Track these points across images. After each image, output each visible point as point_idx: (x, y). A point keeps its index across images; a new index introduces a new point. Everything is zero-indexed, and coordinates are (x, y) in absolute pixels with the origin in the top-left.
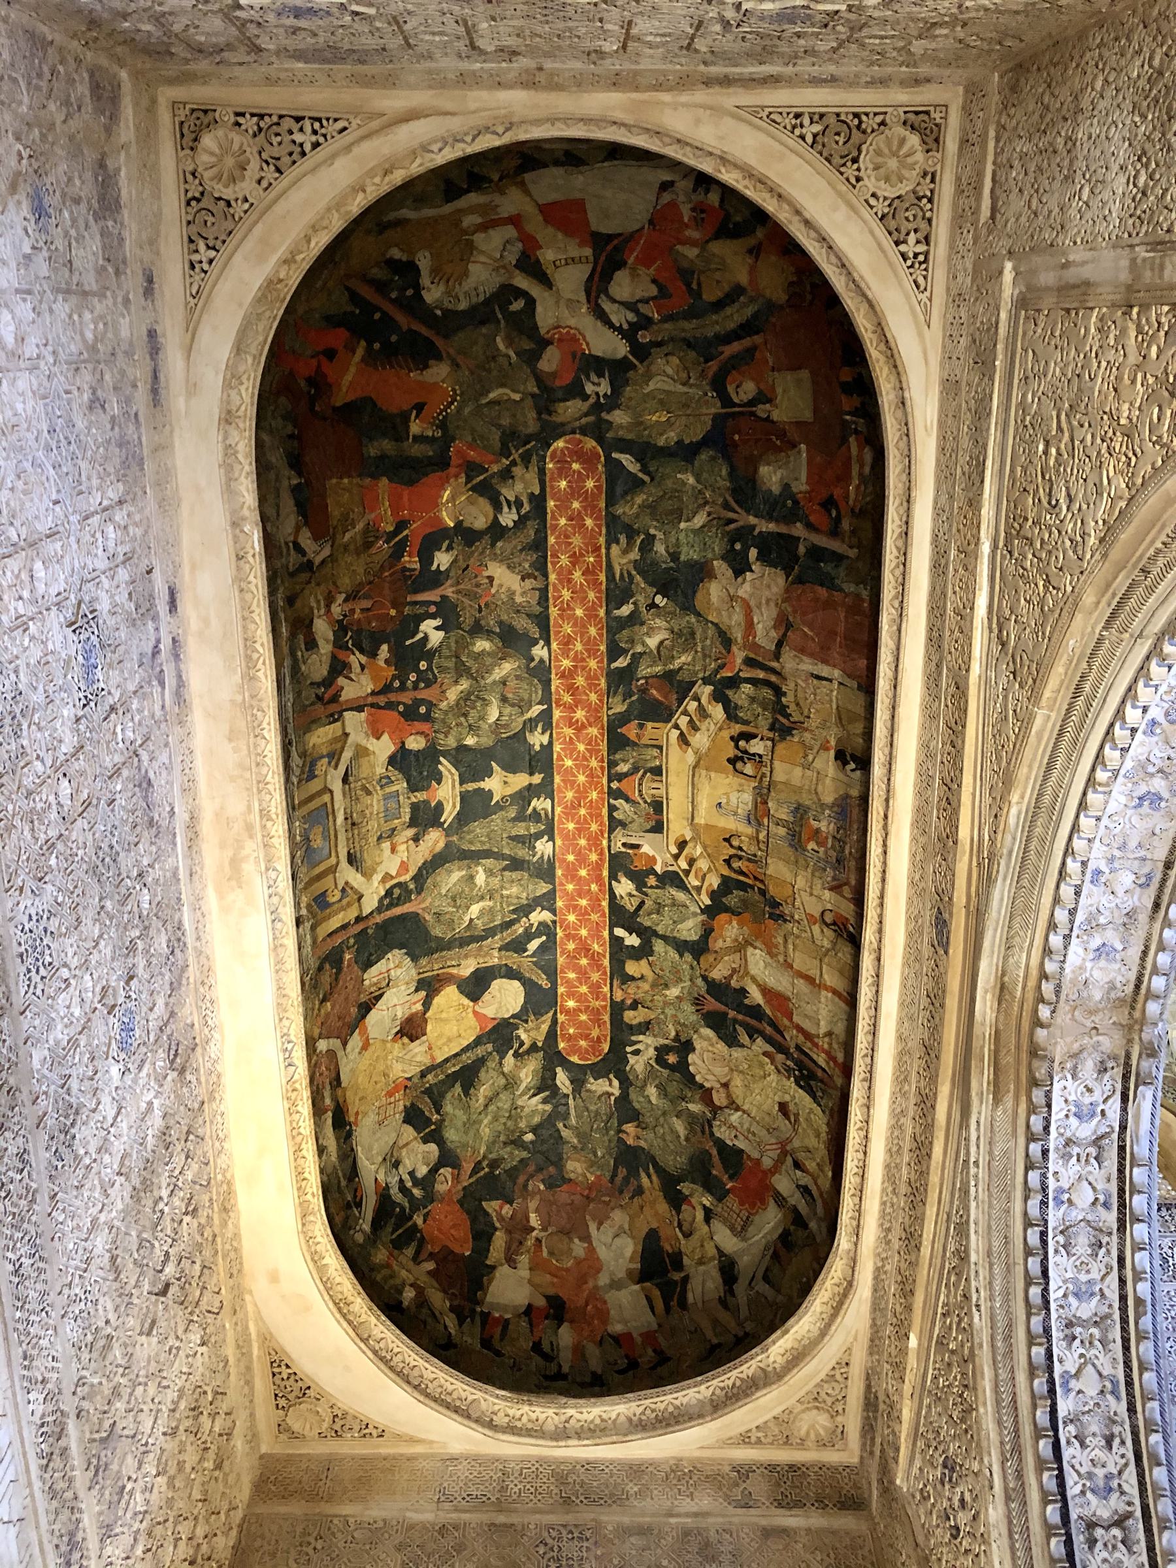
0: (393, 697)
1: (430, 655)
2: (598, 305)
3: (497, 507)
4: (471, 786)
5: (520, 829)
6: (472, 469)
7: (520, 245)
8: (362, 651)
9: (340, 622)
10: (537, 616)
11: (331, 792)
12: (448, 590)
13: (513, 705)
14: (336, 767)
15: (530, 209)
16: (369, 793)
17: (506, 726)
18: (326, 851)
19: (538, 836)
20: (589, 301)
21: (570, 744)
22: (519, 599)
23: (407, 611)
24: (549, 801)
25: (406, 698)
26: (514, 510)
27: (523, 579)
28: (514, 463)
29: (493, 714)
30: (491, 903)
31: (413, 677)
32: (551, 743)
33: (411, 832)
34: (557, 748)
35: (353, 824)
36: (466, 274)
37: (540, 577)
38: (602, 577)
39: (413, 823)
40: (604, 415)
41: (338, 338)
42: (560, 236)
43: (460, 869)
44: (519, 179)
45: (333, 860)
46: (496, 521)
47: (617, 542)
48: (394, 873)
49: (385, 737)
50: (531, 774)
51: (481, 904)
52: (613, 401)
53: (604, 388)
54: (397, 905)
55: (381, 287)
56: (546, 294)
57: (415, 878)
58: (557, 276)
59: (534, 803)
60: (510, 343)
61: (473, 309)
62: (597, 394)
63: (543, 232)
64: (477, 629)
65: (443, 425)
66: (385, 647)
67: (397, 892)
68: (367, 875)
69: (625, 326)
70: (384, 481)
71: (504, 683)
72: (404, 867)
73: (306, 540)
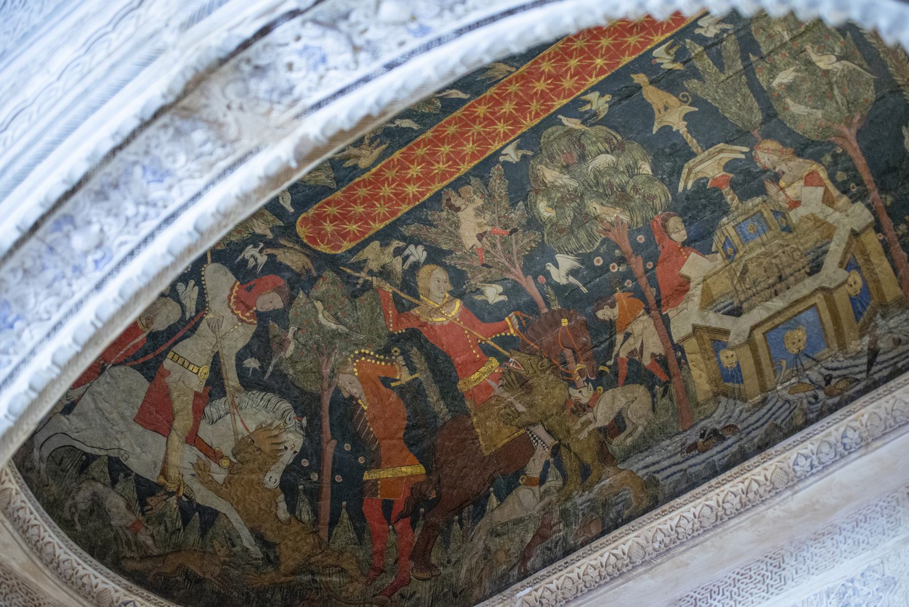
0: (643, 281)
1: (585, 259)
2: (197, 311)
3: (416, 266)
4: (693, 143)
5: (705, 64)
6: (402, 308)
7: (207, 409)
8: (612, 345)
9: (596, 384)
10: (482, 177)
11: (753, 329)
12: (517, 273)
13: (583, 147)
14: (726, 333)
15: (175, 439)
16: (745, 271)
17: (607, 140)
18: (810, 315)
19: (701, 39)
20: (202, 318)
21: (581, 73)
22: (479, 202)
23: (556, 306)
24: (655, 53)
25: (637, 265)
26: (407, 252)
27: (458, 209)
28: (371, 273)
29: (604, 160)
30: (808, 47)
31: (615, 268)
32: (593, 89)
33: (772, 189)
34: (593, 81)
35: (780, 279)
36: (260, 428)
37: (445, 197)
38: (397, 155)
39: (761, 191)
40: (270, 236)
41: (372, 508)
42: (175, 394)
43: (786, 108)
44: (162, 480)
45: (819, 299)
46: (429, 260)
47: (355, 167)
48: (820, 190)
49: (685, 270)
50: (639, 88)
51: (814, 58)
52: (255, 239)
53: (250, 252)
54: (855, 169)
55: (314, 495)
56: (225, 352)
57: (817, 158)
58: (204, 362)
59: (667, 66)
60: (282, 345)
61: (283, 395)
62: (260, 252)
63: (182, 403)
64: (533, 223)
65: (386, 351)
66: (600, 314)
67: (841, 176)
68: (828, 231)
69: (192, 283)
70: (461, 385)
71: (566, 168)
72: (810, 180)
73: (534, 468)
